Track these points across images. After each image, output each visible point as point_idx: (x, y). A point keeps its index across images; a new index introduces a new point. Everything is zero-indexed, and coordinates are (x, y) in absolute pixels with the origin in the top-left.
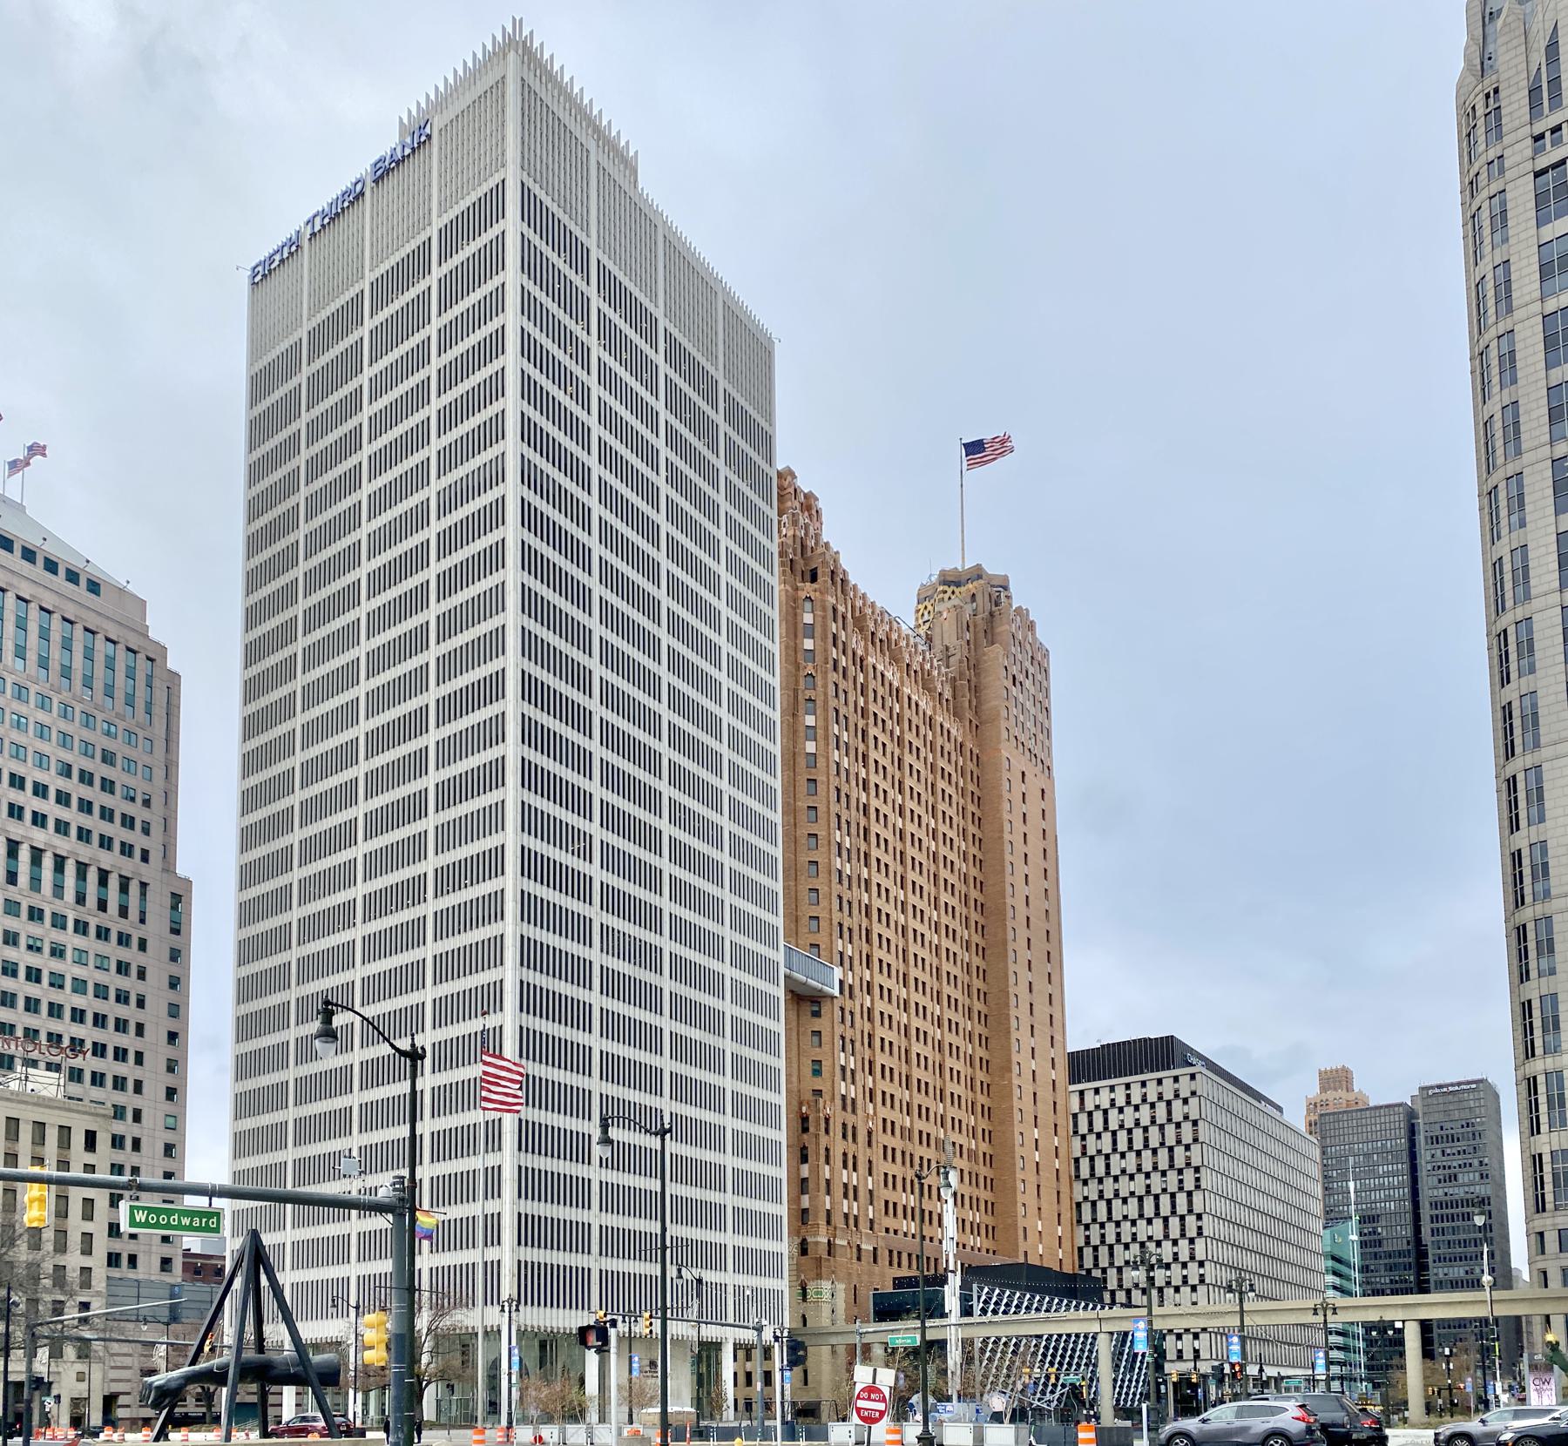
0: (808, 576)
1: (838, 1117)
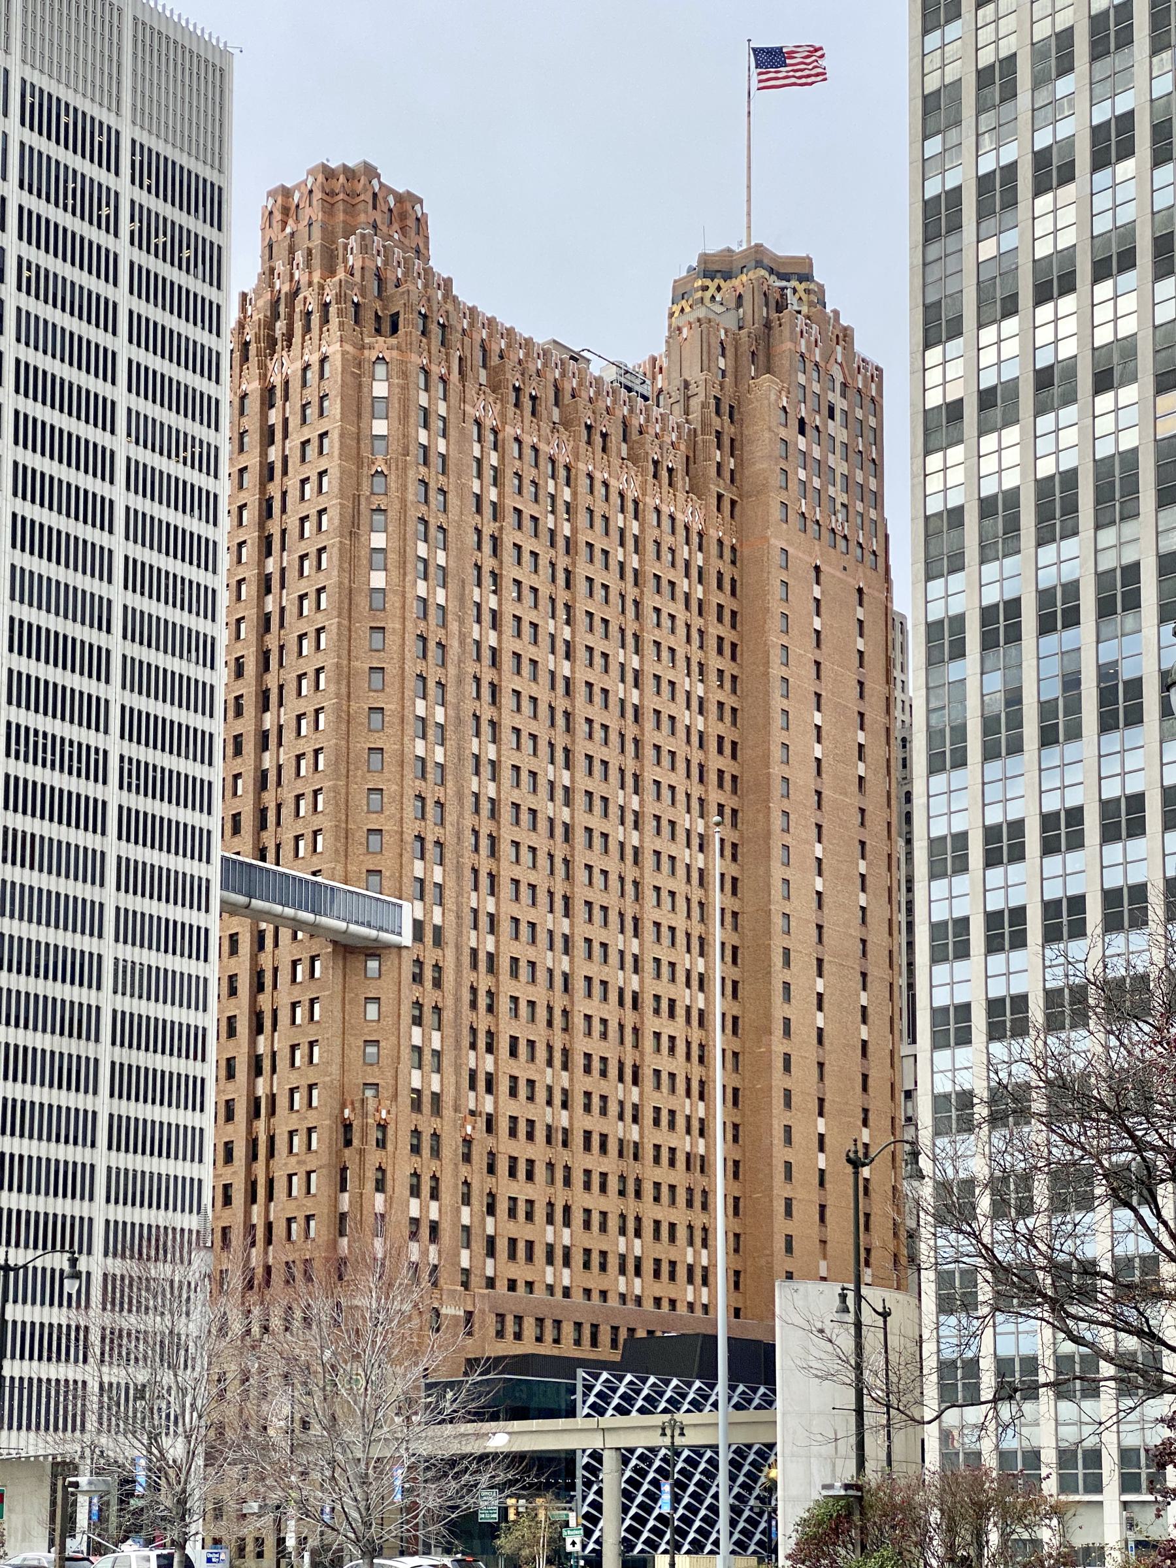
0: (386, 326)
1: (402, 1122)
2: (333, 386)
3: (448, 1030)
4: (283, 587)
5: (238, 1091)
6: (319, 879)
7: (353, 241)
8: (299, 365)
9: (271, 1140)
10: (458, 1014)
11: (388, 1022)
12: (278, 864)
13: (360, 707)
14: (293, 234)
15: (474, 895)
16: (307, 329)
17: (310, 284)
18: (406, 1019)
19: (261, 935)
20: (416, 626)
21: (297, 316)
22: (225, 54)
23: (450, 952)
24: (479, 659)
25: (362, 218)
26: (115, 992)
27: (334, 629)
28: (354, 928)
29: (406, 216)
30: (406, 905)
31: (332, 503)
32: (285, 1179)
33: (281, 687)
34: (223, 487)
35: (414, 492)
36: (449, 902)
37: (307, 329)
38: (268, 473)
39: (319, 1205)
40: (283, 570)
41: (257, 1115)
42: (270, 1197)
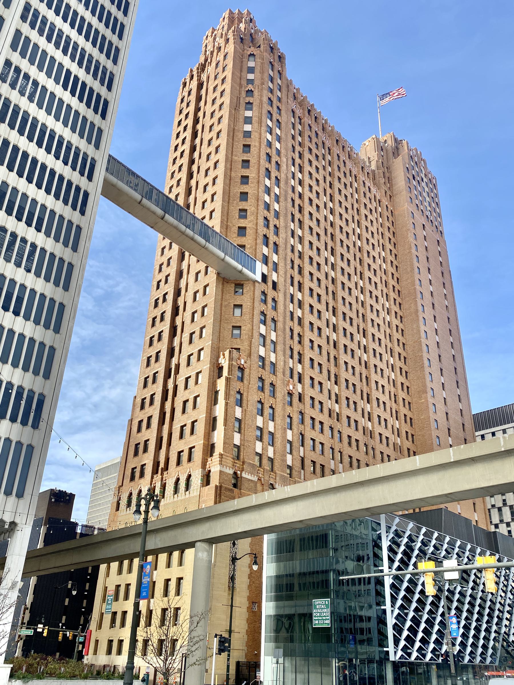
11: (247, 317)
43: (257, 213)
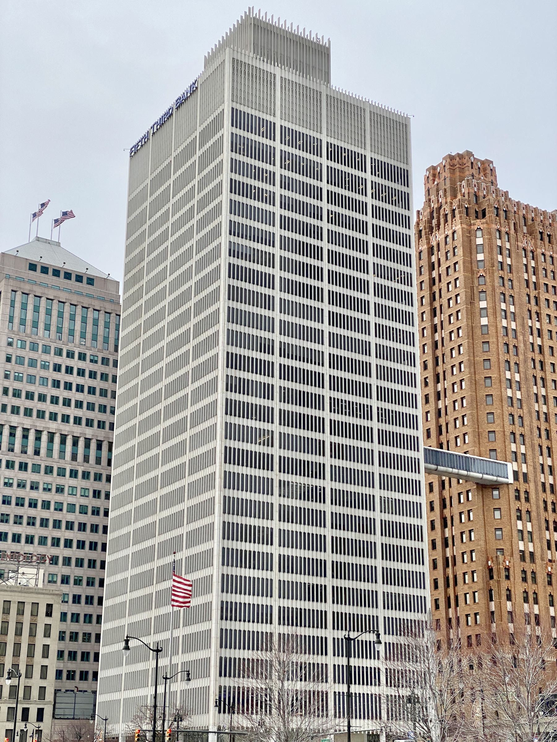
0: (480, 215)
2: (459, 242)
3: (534, 521)
4: (442, 329)
5: (438, 555)
6: (468, 455)
7: (464, 183)
8: (443, 236)
9: (455, 577)
10: (538, 514)
11: (505, 519)
12: (448, 450)
13: (480, 377)
14: (438, 184)
15: (541, 457)
16: (446, 221)
17: (446, 203)
18: (514, 517)
19: (443, 482)
20: (503, 340)
21: (441, 217)
22: (407, 119)
23: (532, 485)
24: (533, 351)
25: (467, 173)
26: (381, 512)
27: (466, 344)
28: (485, 476)
29: (486, 169)
30: (509, 465)
31: (462, 291)
32: (463, 596)
33: (444, 372)
34: (414, 290)
35: (497, 282)
36: (529, 461)
37: (446, 221)
38: (433, 282)
39: (480, 608)
40: (442, 322)
41: (448, 566)
42: (457, 605)
43: (503, 415)
